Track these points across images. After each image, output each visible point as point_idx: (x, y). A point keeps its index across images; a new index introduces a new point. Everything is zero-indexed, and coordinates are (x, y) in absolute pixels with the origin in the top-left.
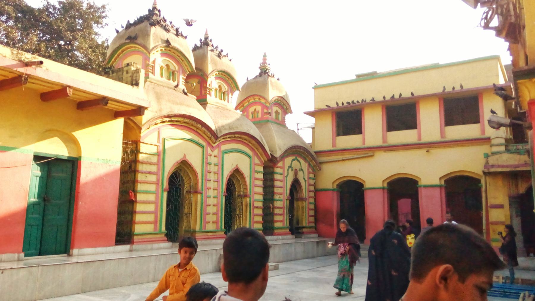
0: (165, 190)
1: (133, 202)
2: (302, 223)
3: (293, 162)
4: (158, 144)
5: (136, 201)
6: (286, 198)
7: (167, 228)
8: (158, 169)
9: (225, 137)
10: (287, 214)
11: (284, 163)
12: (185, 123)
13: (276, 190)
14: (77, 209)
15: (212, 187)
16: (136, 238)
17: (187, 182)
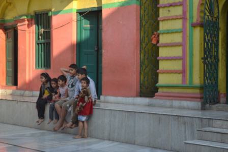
0: (194, 26)
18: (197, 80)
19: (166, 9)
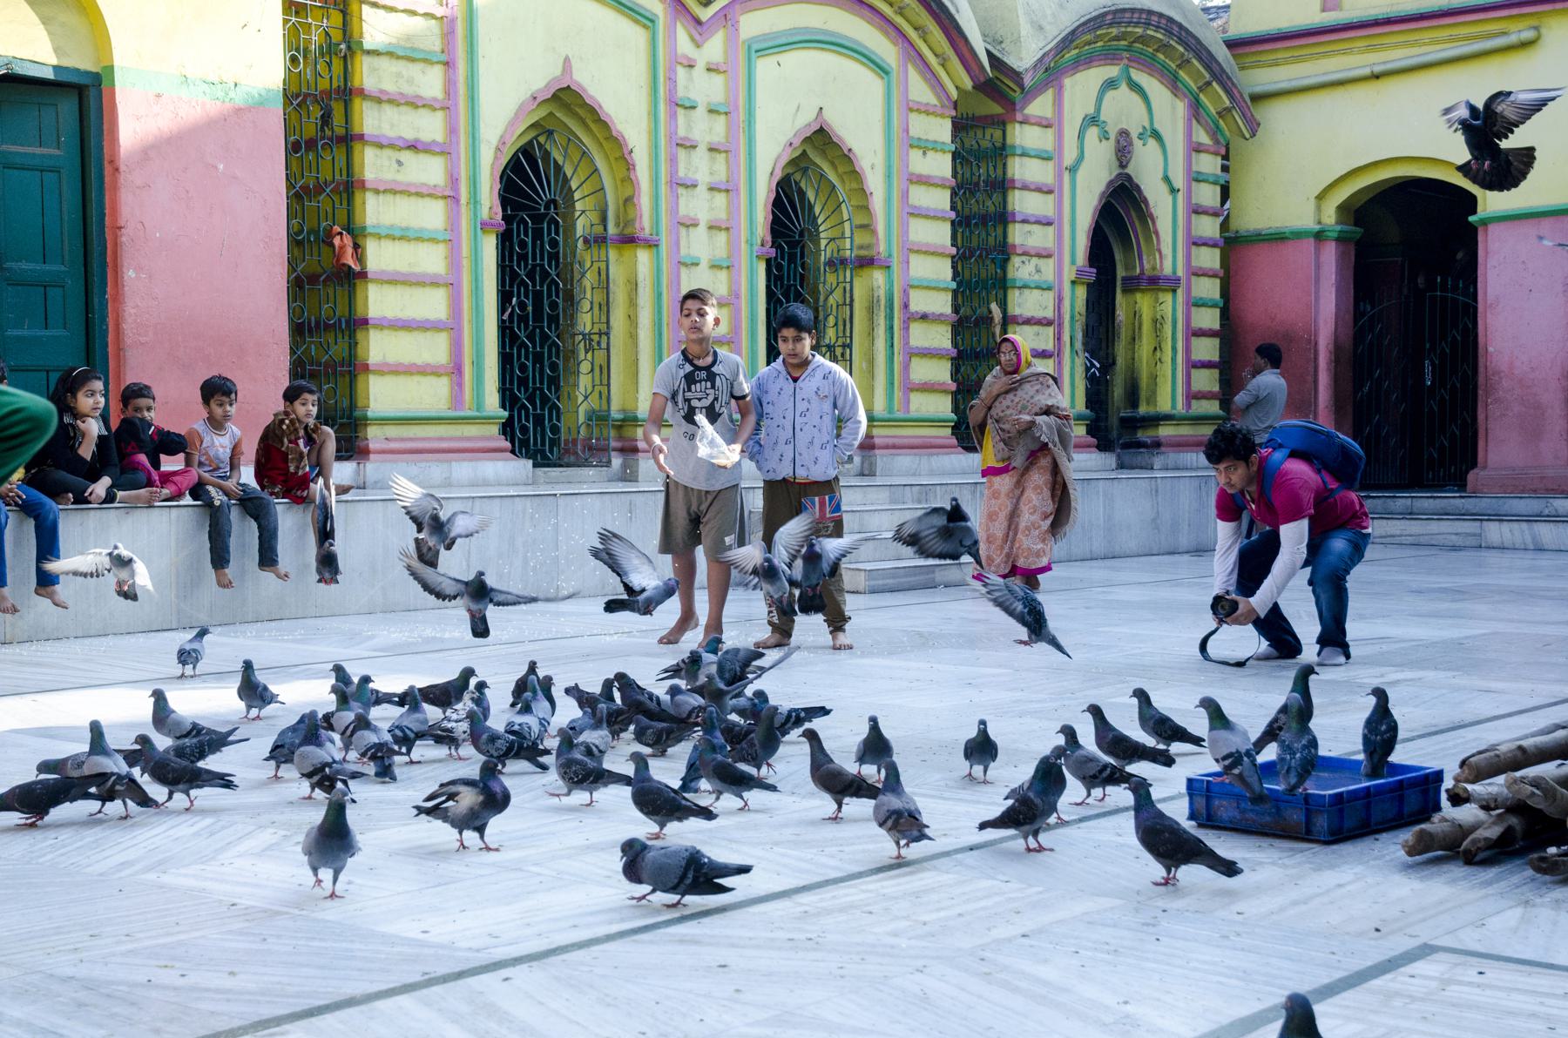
0: (485, 226)
1: (351, 278)
2: (1152, 399)
3: (1110, 94)
4: (439, 12)
5: (363, 275)
6: (1069, 274)
7: (508, 397)
8: (452, 130)
10: (1074, 352)
11: (1058, 102)
13: (1018, 235)
14: (118, 297)
15: (703, 217)
16: (374, 436)
17: (586, 189)
18: (492, 400)
19: (387, 152)
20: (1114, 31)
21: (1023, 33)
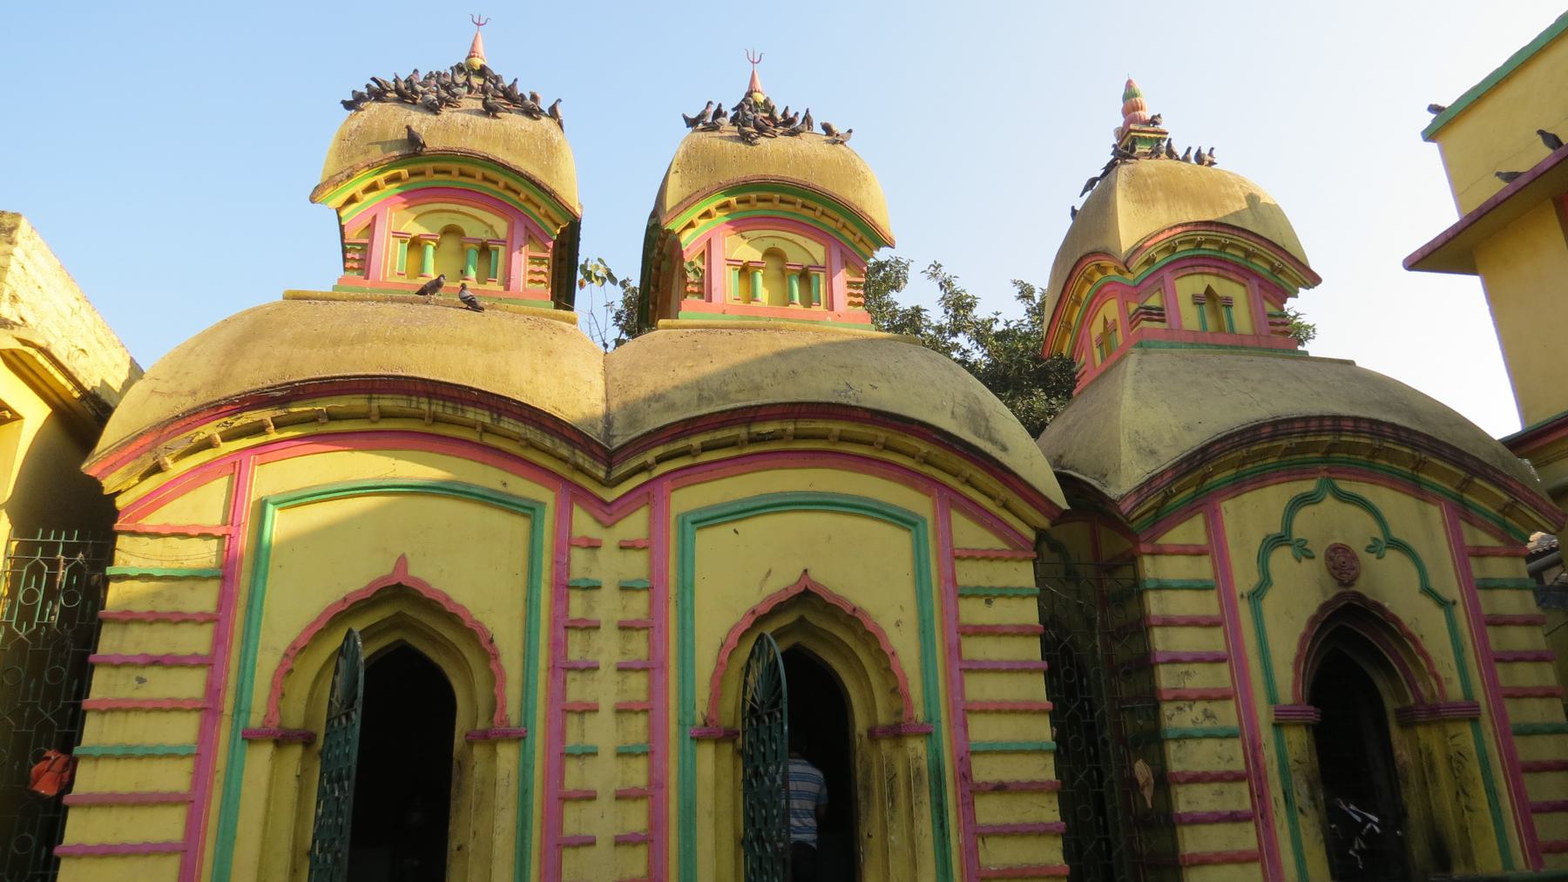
2: (1468, 859)
6: (1264, 716)
9: (680, 445)
11: (1214, 527)
12: (385, 415)
19: (123, 671)
20: (1284, 443)
21: (1124, 460)
